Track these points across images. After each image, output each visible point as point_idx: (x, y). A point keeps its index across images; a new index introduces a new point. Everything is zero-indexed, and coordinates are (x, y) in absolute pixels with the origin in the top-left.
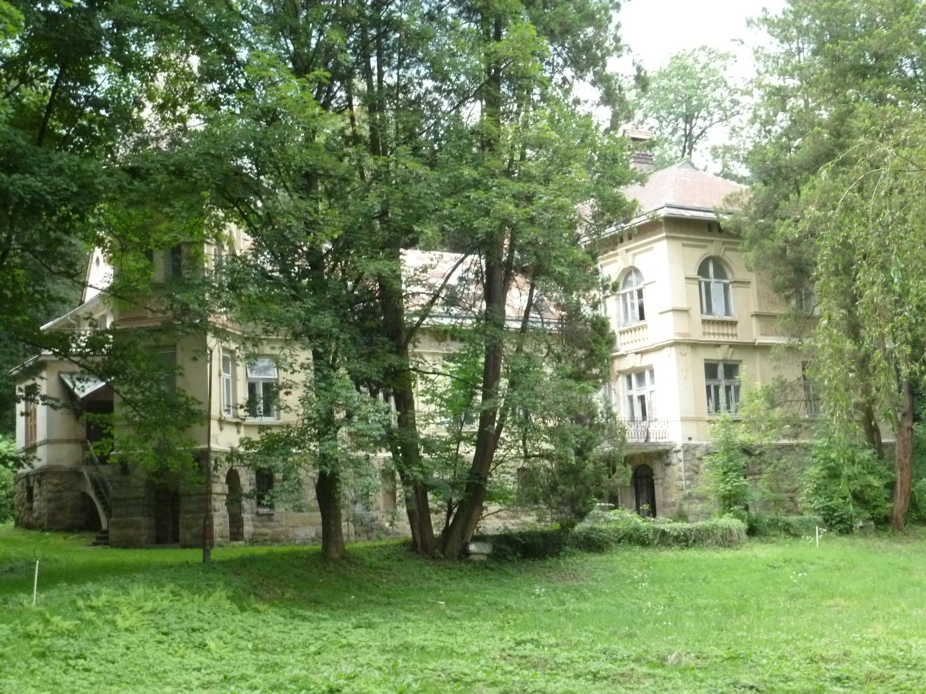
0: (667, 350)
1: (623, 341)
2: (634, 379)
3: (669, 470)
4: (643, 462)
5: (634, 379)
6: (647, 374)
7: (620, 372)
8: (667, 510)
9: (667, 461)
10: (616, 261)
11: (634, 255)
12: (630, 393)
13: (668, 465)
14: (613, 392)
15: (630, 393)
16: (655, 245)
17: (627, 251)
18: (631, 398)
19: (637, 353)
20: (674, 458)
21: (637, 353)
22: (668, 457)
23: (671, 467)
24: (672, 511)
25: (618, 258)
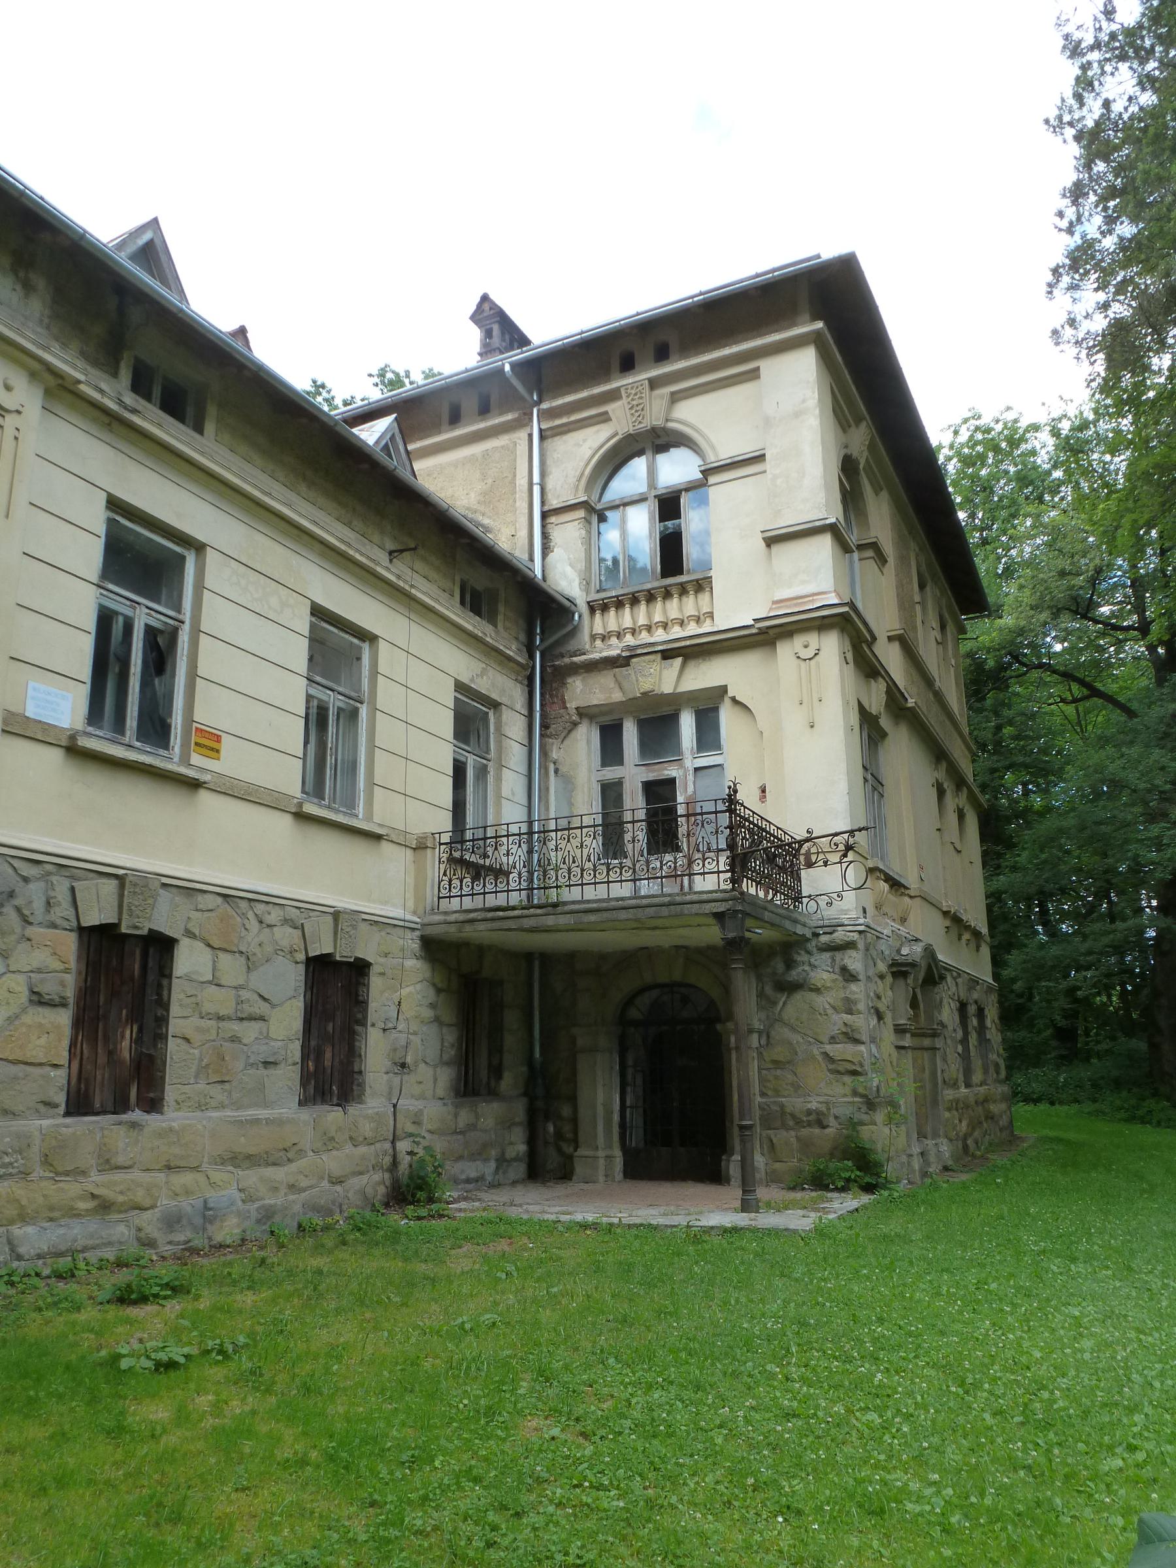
0: (813, 639)
1: (598, 628)
2: (630, 734)
3: (793, 1007)
4: (677, 976)
5: (630, 734)
6: (687, 724)
7: (583, 713)
8: (785, 1138)
9: (794, 975)
10: (604, 418)
11: (675, 398)
12: (611, 773)
13: (792, 988)
14: (552, 767)
15: (611, 773)
16: (767, 366)
17: (654, 384)
18: (611, 793)
19: (667, 655)
20: (821, 971)
21: (667, 655)
22: (790, 964)
23: (798, 996)
24: (806, 1145)
25: (611, 408)
